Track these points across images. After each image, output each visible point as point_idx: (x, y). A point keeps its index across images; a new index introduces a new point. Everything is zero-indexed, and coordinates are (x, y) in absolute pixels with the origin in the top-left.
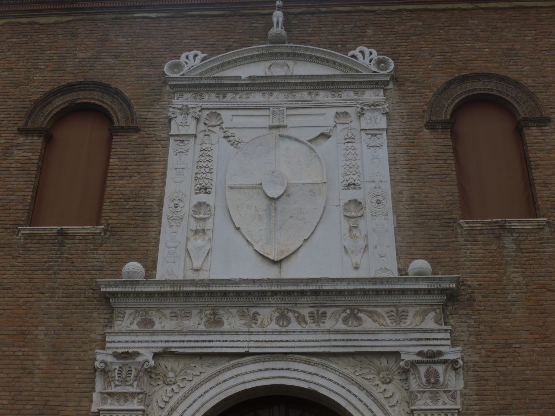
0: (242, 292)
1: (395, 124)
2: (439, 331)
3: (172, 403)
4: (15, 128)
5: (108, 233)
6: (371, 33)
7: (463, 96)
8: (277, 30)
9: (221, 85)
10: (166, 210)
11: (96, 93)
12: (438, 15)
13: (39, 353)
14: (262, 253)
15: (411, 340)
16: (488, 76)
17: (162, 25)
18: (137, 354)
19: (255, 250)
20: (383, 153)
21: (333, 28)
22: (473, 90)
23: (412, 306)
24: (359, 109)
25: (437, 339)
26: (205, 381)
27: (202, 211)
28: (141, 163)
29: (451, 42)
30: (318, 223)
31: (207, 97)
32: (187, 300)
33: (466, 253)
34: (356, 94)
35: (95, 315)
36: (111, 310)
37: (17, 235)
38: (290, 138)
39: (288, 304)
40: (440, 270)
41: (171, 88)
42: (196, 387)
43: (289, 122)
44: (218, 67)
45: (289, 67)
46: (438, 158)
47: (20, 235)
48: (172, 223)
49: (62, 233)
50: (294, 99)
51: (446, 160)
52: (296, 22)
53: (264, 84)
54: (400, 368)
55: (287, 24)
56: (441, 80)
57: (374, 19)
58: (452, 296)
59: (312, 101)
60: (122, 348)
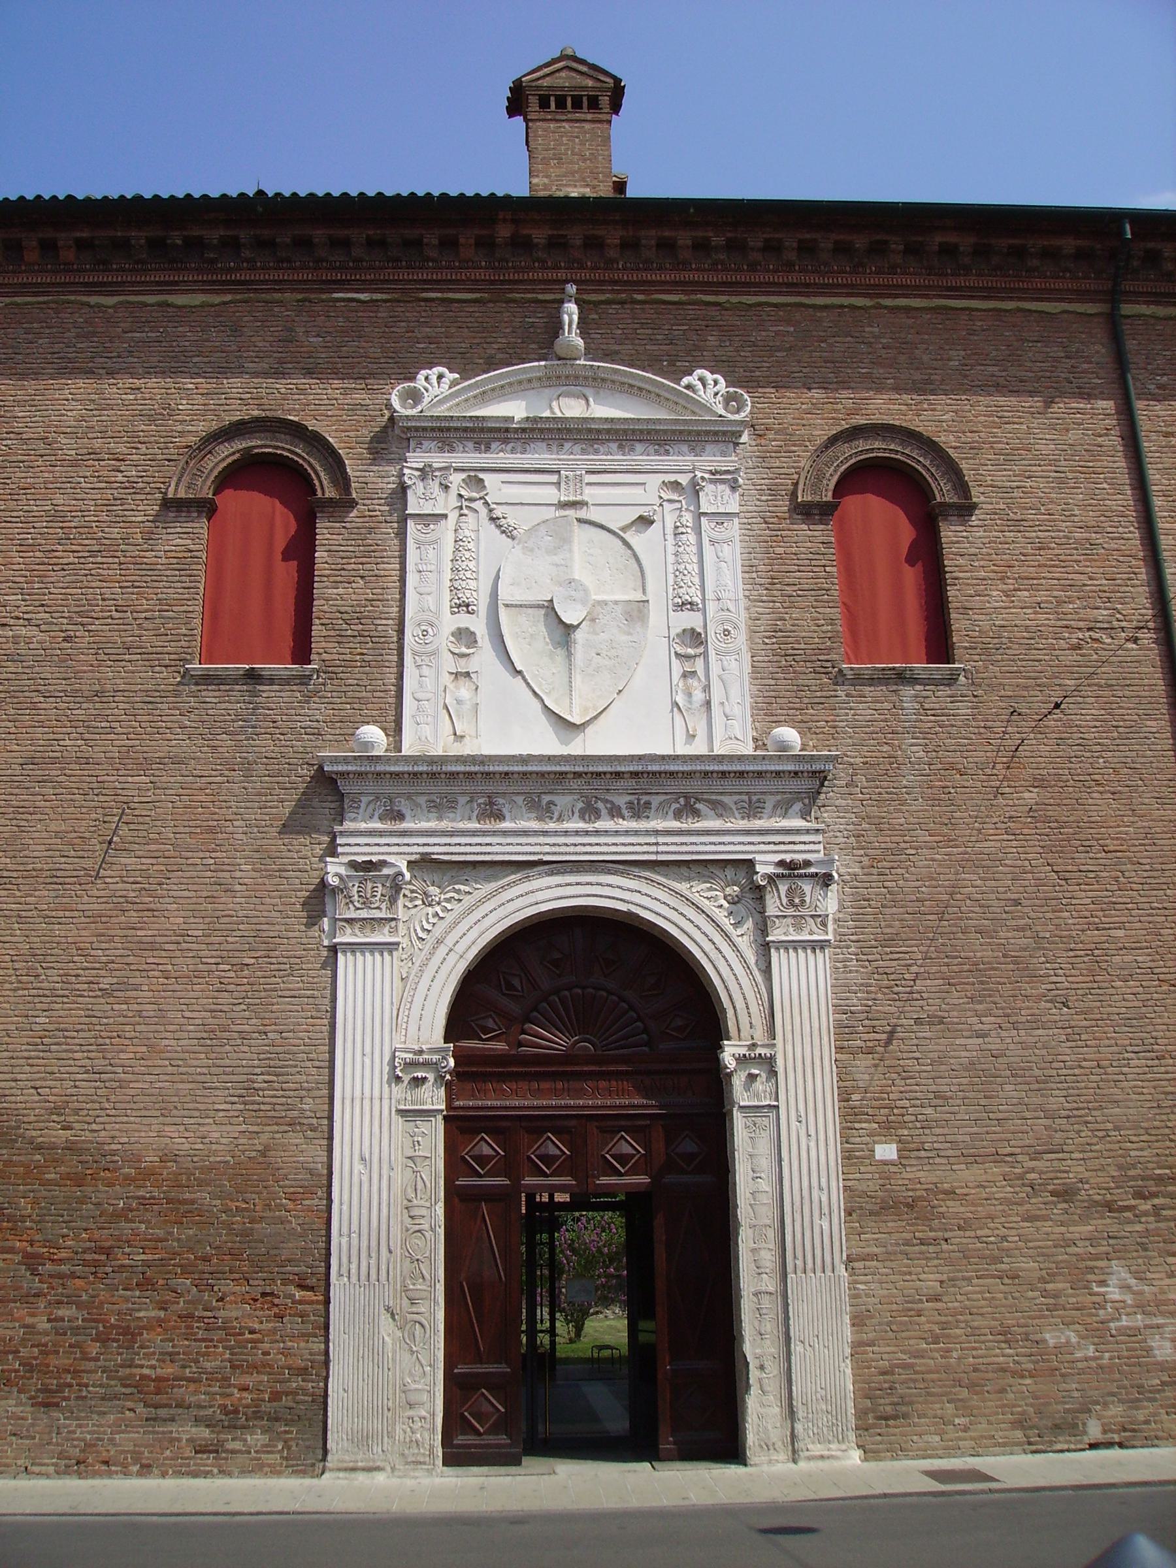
9: (482, 430)
15: (769, 843)
18: (384, 863)
23: (771, 793)
25: (805, 843)
26: (481, 902)
28: (364, 560)
33: (847, 715)
35: (316, 803)
42: (470, 910)
43: (589, 494)
46: (813, 562)
52: (596, 317)
56: (822, 434)
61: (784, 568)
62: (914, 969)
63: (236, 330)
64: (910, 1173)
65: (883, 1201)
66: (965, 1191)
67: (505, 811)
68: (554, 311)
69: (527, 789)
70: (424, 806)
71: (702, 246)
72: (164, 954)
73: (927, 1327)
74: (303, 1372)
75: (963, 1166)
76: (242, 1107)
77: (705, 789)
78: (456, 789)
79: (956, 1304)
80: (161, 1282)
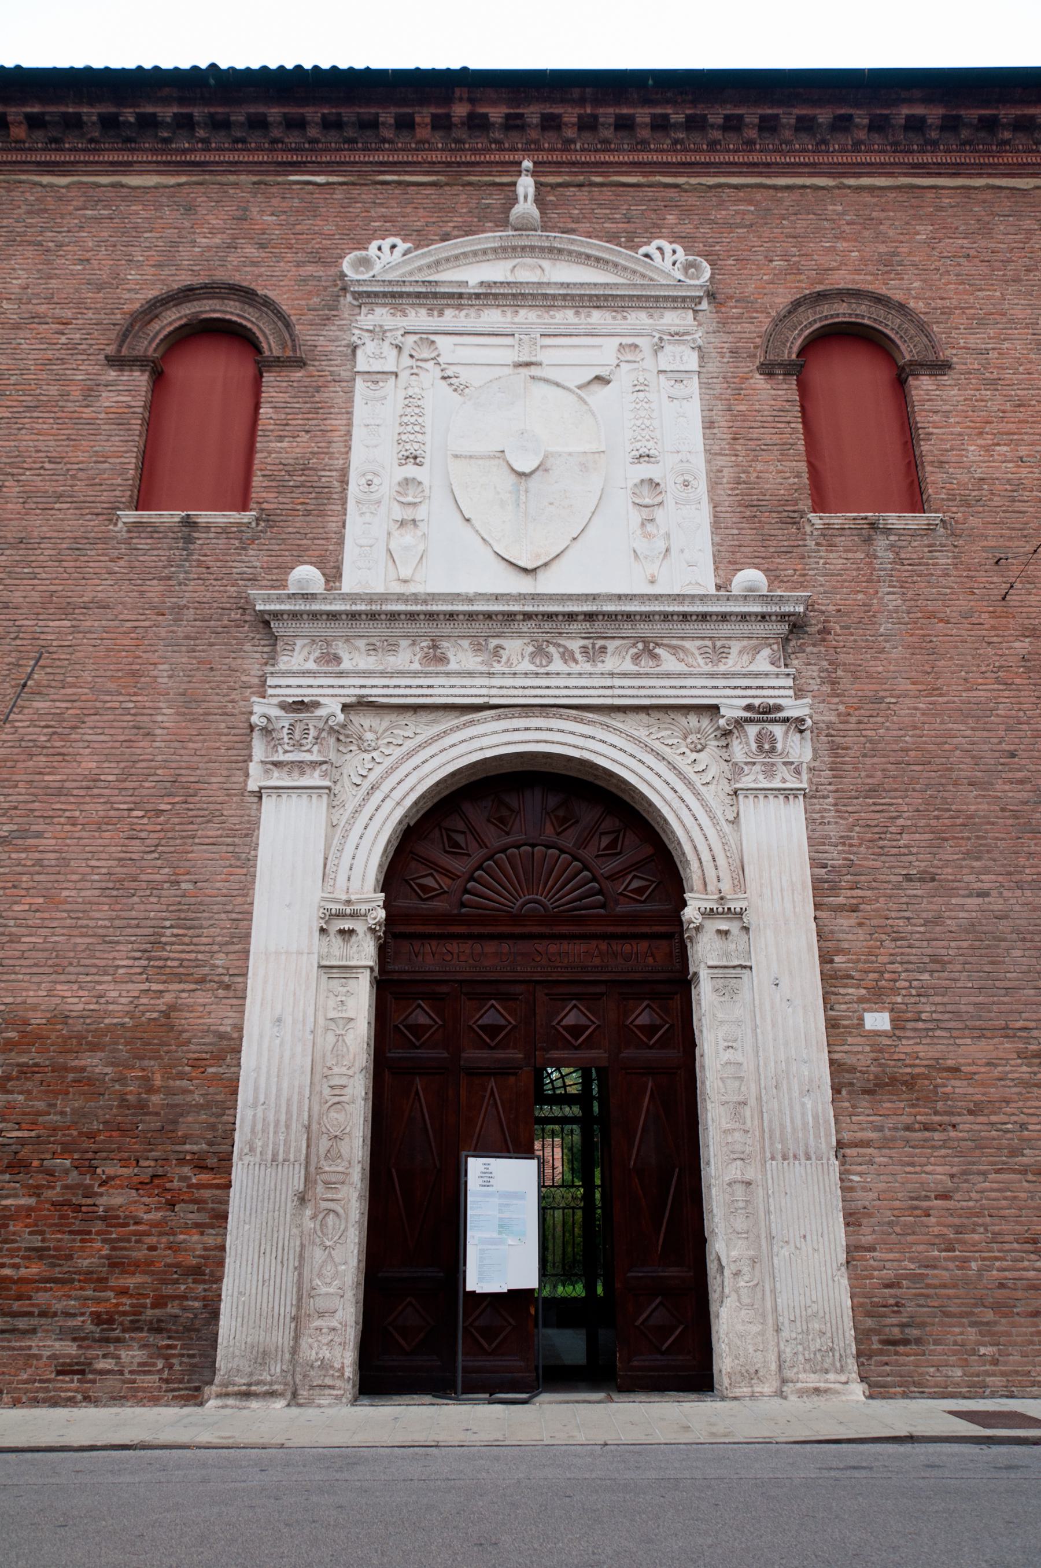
0: (478, 613)
2: (777, 675)
3: (372, 777)
4: (102, 357)
5: (262, 524)
8: (526, 207)
9: (435, 295)
11: (232, 303)
13: (161, 705)
15: (735, 688)
16: (856, 294)
18: (316, 705)
20: (694, 410)
22: (832, 316)
23: (737, 639)
24: (656, 340)
25: (774, 688)
26: (421, 746)
27: (411, 492)
35: (248, 647)
36: (274, 639)
37: (116, 525)
38: (546, 381)
41: (355, 299)
42: (410, 755)
44: (429, 267)
47: (120, 524)
48: (364, 510)
49: (188, 523)
52: (553, 198)
53: (504, 296)
54: (718, 728)
55: (539, 201)
56: (783, 299)
58: (796, 625)
60: (293, 695)
61: (746, 424)
62: (900, 822)
63: (190, 209)
64: (906, 1046)
65: (877, 1077)
66: (973, 1069)
67: (450, 655)
69: (473, 632)
70: (363, 648)
71: (661, 125)
72: (72, 799)
73: (936, 1230)
74: (196, 1272)
75: (969, 1041)
76: (144, 963)
77: (665, 633)
78: (397, 632)
79: (971, 1204)
80: (36, 1163)
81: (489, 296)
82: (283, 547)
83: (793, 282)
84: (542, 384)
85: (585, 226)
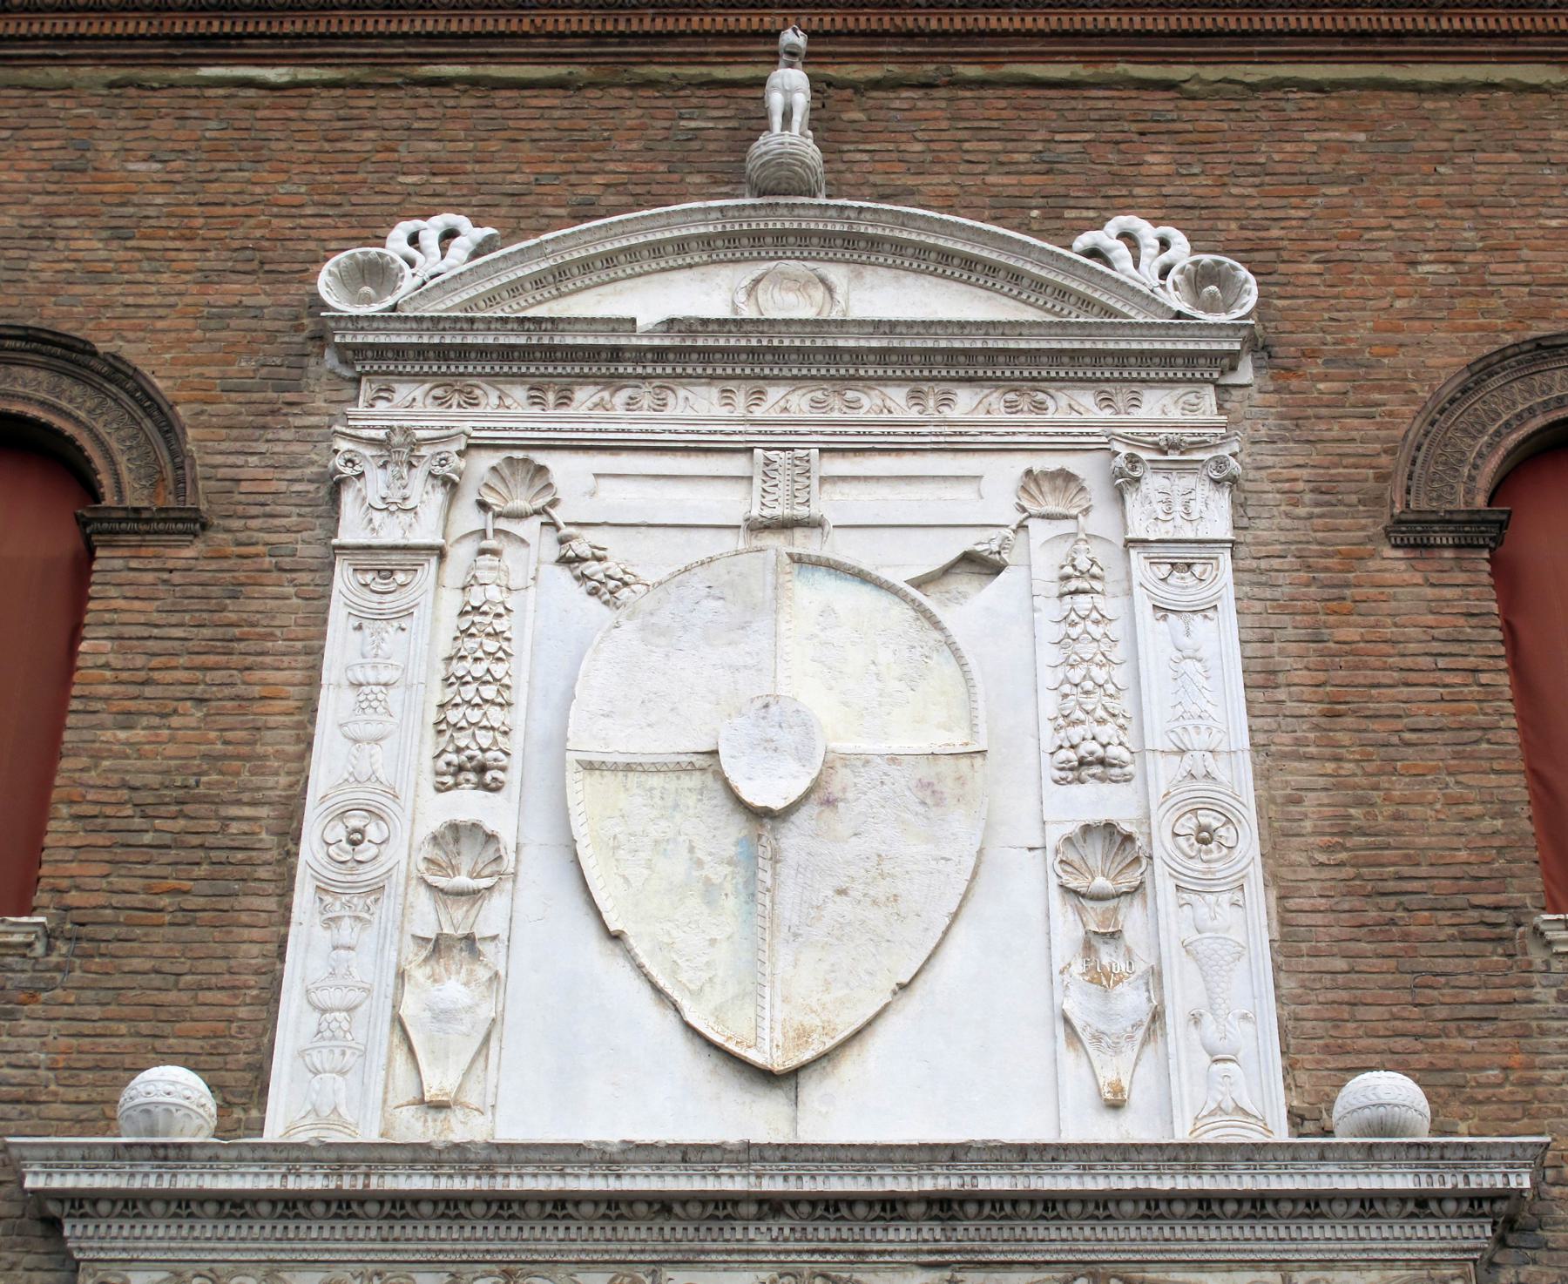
1: (1264, 523)
6: (1164, 169)
7: (1538, 422)
9: (551, 353)
10: (310, 851)
11: (30, 373)
12: (1428, 105)
14: (718, 1039)
17: (311, 114)
19: (688, 1027)
20: (1220, 641)
21: (1010, 146)
24: (1120, 461)
27: (465, 862)
28: (211, 659)
29: (1483, 211)
30: (955, 916)
31: (494, 400)
32: (397, 1232)
34: (1107, 401)
39: (827, 1251)
40: (1464, 1118)
41: (344, 362)
43: (826, 504)
44: (538, 281)
45: (830, 289)
46: (1442, 662)
48: (337, 909)
50: (852, 415)
51: (1475, 671)
55: (822, 122)
56: (1445, 355)
57: (1174, 115)
59: (924, 424)
61: (1361, 677)
68: (751, 105)
69: (619, 1250)
81: (689, 353)
82: (113, 1009)
83: (1473, 314)
84: (820, 576)
85: (940, 180)
